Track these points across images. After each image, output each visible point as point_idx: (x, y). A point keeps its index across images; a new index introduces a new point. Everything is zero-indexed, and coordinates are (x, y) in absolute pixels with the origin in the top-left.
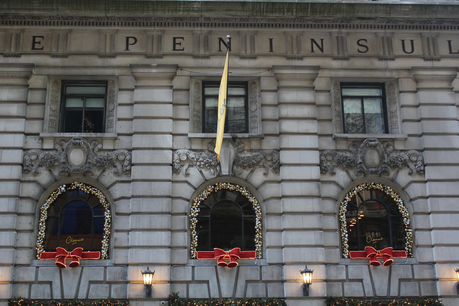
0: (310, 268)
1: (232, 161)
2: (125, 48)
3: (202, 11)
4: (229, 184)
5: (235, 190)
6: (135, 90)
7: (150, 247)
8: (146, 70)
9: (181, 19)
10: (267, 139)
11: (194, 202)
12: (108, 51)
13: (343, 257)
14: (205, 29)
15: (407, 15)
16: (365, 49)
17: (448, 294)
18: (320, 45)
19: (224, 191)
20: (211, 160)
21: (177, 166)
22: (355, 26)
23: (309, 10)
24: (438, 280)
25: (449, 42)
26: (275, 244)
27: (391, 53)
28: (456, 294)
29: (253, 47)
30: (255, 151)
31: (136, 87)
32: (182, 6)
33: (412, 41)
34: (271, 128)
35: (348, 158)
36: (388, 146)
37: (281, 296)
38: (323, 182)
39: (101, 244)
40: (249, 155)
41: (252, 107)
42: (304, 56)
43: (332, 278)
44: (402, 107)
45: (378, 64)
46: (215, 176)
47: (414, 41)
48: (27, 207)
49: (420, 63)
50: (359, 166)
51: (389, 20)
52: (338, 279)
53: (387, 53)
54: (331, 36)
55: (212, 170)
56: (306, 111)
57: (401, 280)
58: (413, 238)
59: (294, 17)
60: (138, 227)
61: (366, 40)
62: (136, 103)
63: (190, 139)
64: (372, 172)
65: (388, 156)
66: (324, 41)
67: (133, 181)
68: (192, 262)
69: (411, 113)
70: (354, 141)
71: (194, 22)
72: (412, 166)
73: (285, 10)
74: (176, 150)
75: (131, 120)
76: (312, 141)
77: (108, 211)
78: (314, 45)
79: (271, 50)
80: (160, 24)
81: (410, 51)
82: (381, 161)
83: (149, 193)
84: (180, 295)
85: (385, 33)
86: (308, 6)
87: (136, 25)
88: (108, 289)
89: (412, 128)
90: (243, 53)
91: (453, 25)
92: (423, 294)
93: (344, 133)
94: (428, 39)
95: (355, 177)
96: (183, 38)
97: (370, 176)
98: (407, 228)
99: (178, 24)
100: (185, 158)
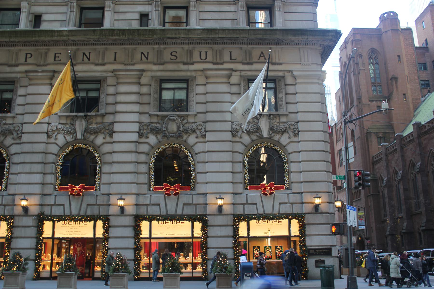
0: (123, 197)
1: (84, 130)
2: (24, 60)
3: (68, 36)
4: (82, 145)
5: (86, 148)
6: (28, 87)
7: (30, 184)
8: (35, 74)
9: (57, 41)
10: (107, 116)
11: (60, 156)
12: (13, 62)
13: (150, 190)
14: (74, 47)
16: (175, 58)
17: (213, 213)
18: (146, 56)
19: (80, 149)
20: (71, 130)
21: (50, 133)
22: (169, 43)
23: (136, 34)
24: (208, 204)
25: (231, 52)
26: (107, 182)
27: (191, 60)
28: (218, 213)
29: (103, 58)
30: (100, 123)
31: (30, 85)
32: (56, 33)
33: (206, 52)
34: (110, 109)
36: (183, 120)
37: (108, 214)
39: (2, 182)
40: (95, 126)
41: (191, 95)
43: (141, 203)
44: (197, 94)
45: (183, 67)
46: (73, 140)
47: (207, 52)
49: (211, 66)
50: (163, 132)
51: (189, 39)
52: (144, 203)
53: (189, 60)
54: (154, 50)
55: (71, 136)
56: (133, 98)
57: (184, 204)
58: (195, 178)
59: (126, 38)
60: (23, 171)
61: (176, 52)
62: (29, 94)
63: (59, 116)
64: (171, 136)
65: (183, 125)
66: (149, 53)
67: (23, 143)
68: (56, 193)
69: (201, 99)
70: (162, 117)
71: (66, 43)
72: (198, 132)
73: (121, 34)
74: (51, 123)
75: (24, 105)
76: (135, 117)
77: (8, 162)
78: (143, 55)
79: (115, 60)
80: (46, 45)
81: (204, 58)
82: (178, 129)
83: (31, 151)
84: (46, 213)
85: (189, 47)
86: (135, 31)
87: (31, 46)
88: (3, 209)
89: (201, 108)
90: (97, 62)
91: (262, 42)
92: (198, 213)
93: (160, 111)
94: (217, 51)
95: (161, 140)
96: (61, 53)
97: (171, 139)
98: (193, 172)
99: (57, 44)
100: (55, 128)
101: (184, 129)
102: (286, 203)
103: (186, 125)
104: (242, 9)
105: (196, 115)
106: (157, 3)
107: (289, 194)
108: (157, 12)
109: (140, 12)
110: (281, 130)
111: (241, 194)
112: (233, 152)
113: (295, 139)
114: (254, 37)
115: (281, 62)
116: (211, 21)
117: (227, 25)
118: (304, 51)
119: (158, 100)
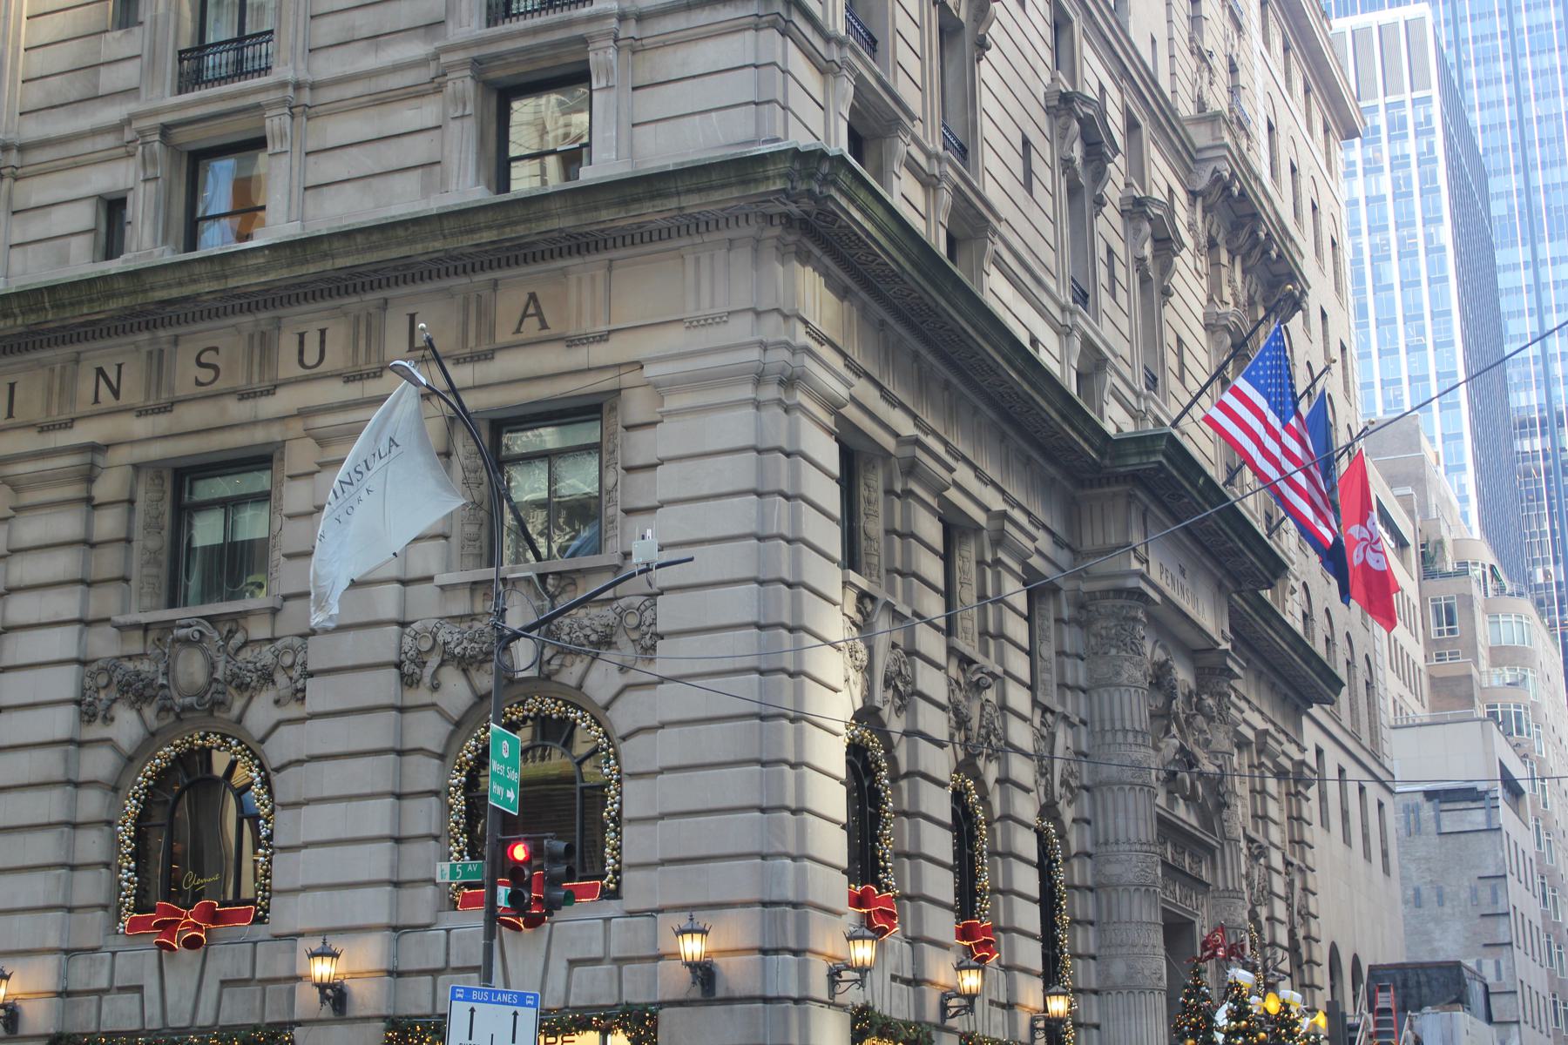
15: (266, 273)
16: (210, 373)
23: (47, 305)
33: (323, 332)
35: (142, 676)
36: (231, 633)
38: (81, 744)
42: (73, 420)
43: (79, 987)
44: (290, 517)
45: (237, 410)
49: (337, 391)
52: (91, 987)
57: (224, 983)
61: (216, 349)
76: (62, 643)
101: (235, 676)
102: (596, 961)
103: (239, 658)
104: (459, 113)
105: (274, 612)
106: (148, 146)
107: (609, 919)
108: (151, 186)
109: (100, 197)
110: (587, 637)
111: (426, 927)
112: (401, 753)
114: (467, 241)
115: (603, 328)
116: (348, 186)
118: (697, 260)
119: (164, 558)
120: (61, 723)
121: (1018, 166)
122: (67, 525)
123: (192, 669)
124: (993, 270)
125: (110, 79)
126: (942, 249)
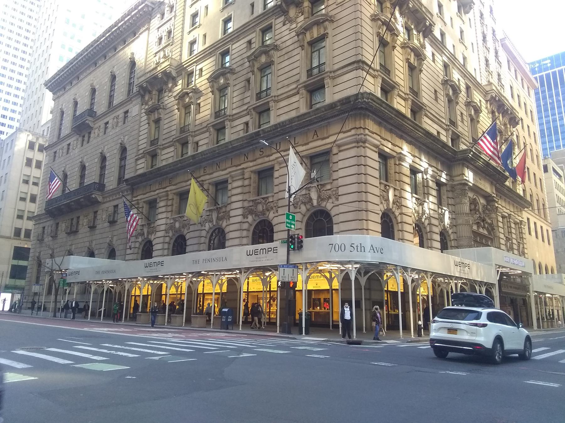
45: (267, 159)
48: (166, 246)
76: (239, 205)
105: (273, 196)
113: (337, 203)
117: (293, 114)
120: (239, 219)
121: (433, 96)
122: (239, 183)
123: (260, 208)
124: (425, 117)
125: (246, 101)
126: (409, 115)
